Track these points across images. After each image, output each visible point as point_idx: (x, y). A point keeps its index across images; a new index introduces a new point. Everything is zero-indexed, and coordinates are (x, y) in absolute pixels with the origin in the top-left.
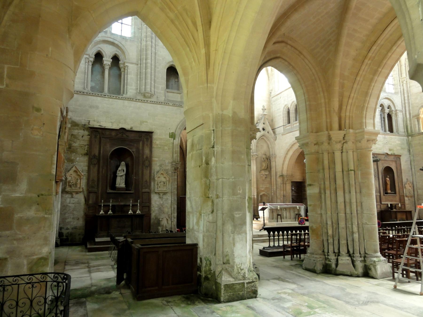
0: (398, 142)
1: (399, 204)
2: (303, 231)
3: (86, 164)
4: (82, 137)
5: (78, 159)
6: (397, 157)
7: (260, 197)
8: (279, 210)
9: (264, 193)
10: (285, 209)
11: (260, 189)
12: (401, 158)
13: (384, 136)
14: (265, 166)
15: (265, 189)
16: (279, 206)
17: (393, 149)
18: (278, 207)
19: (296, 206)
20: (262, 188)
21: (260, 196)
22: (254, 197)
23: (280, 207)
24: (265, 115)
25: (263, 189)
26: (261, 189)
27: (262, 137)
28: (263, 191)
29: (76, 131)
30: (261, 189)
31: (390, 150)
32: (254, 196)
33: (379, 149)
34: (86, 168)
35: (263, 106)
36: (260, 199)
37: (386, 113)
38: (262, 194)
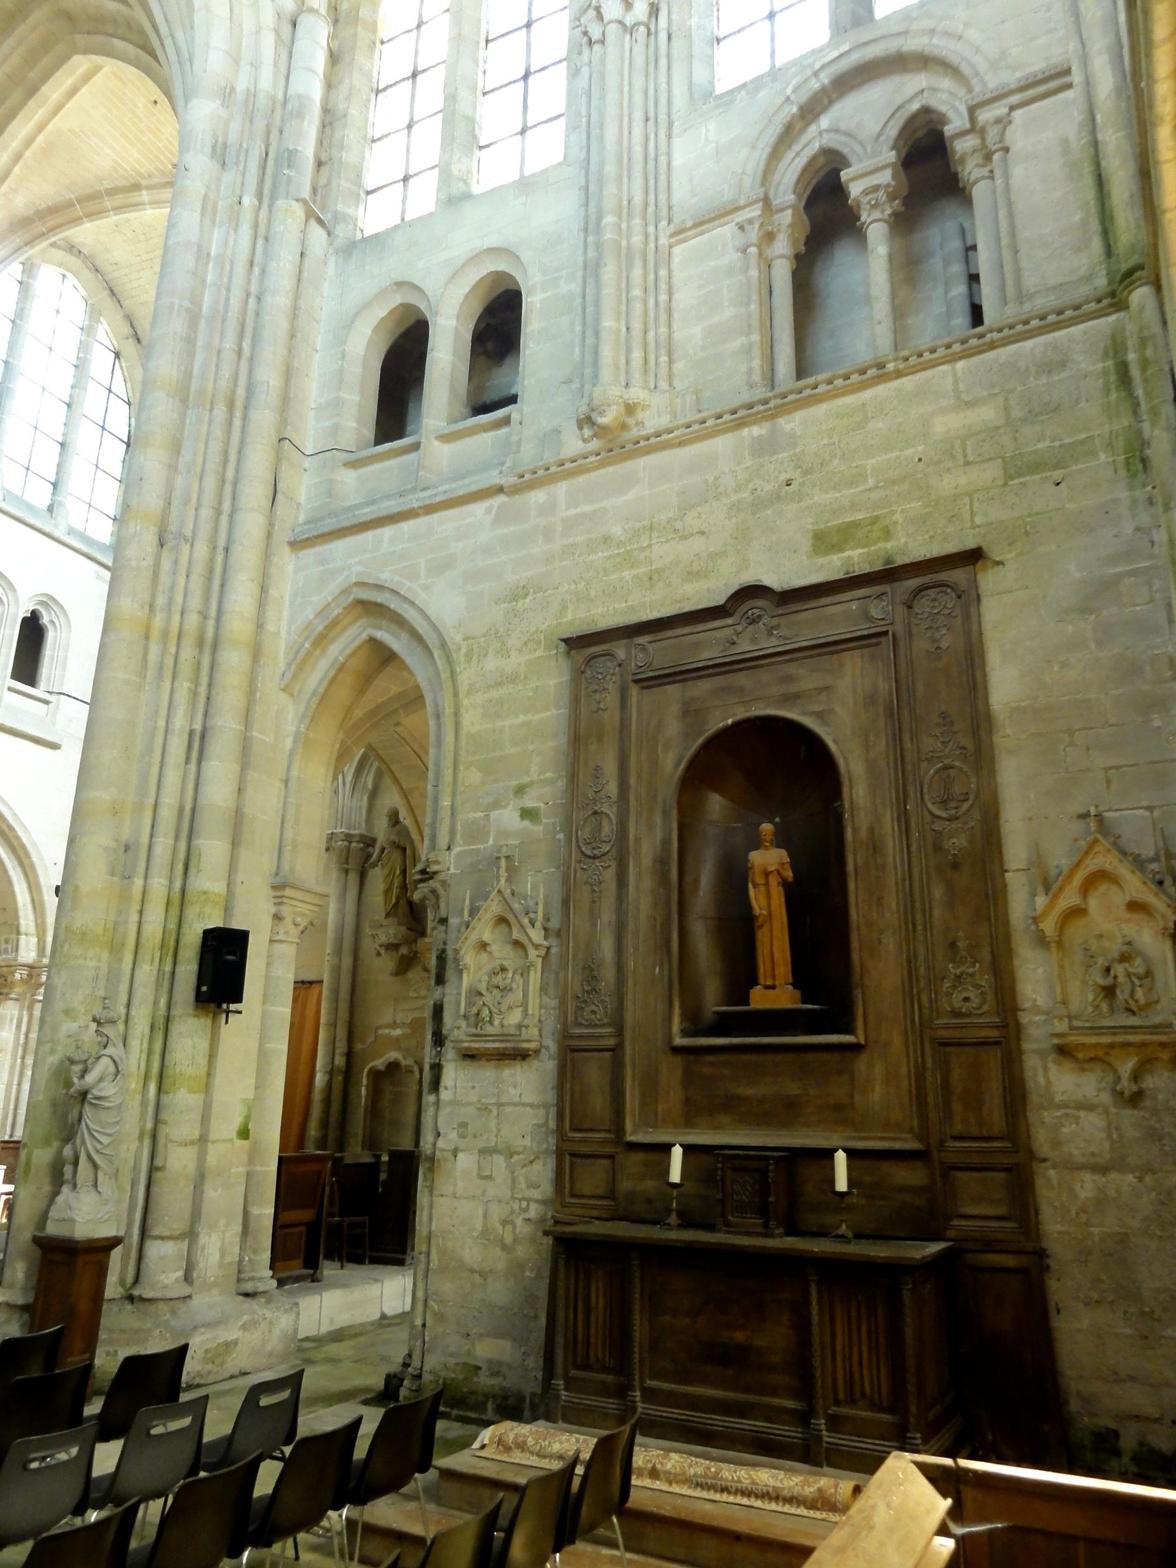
0: (946, 424)
1: (829, 1153)
6: (913, 583)
9: (393, 1055)
11: (380, 1032)
12: (989, 580)
13: (756, 431)
15: (408, 1031)
17: (875, 520)
20: (394, 1025)
25: (398, 1032)
28: (396, 1043)
30: (387, 1031)
31: (824, 542)
33: (691, 576)
37: (865, 200)
38: (379, 1063)
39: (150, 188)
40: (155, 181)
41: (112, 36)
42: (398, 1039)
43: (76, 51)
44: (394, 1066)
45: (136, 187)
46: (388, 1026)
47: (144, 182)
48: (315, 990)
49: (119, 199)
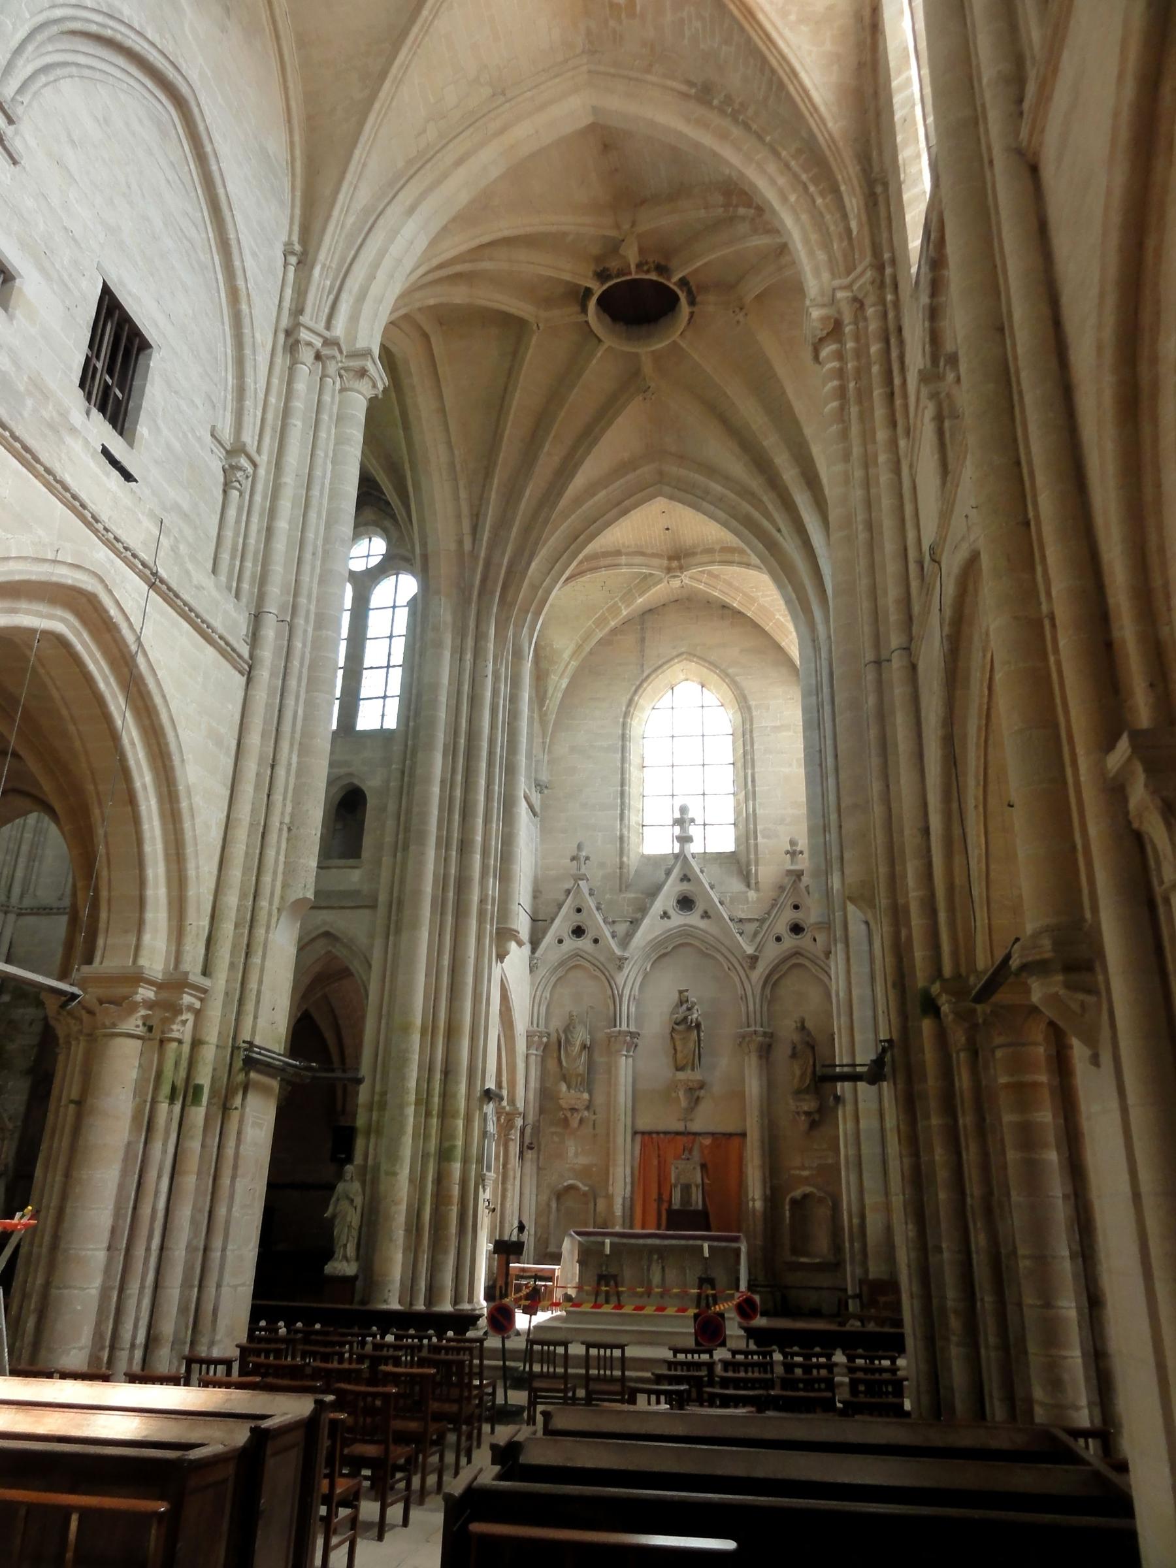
2: (281, 1324)
3: (25, 1097)
4: (31, 1024)
5: (10, 1084)
7: (787, 1207)
8: (607, 1256)
9: (808, 1189)
10: (655, 1257)
11: (792, 1172)
14: (803, 1075)
15: (814, 1172)
16: (608, 1241)
18: (603, 1243)
19: (699, 1242)
20: (803, 1168)
21: (788, 1200)
22: (754, 1206)
23: (611, 1244)
24: (799, 875)
25: (806, 1173)
26: (797, 1172)
27: (794, 961)
28: (806, 1181)
29: (21, 1011)
30: (797, 1172)
32: (754, 1200)
34: (22, 1109)
35: (793, 843)
36: (787, 1214)
38: (797, 1193)
39: (627, 554)
40: (630, 550)
41: (703, 499)
42: (807, 1178)
43: (660, 494)
44: (805, 1196)
45: (618, 553)
46: (799, 1168)
47: (623, 550)
48: (736, 1142)
49: (608, 561)
